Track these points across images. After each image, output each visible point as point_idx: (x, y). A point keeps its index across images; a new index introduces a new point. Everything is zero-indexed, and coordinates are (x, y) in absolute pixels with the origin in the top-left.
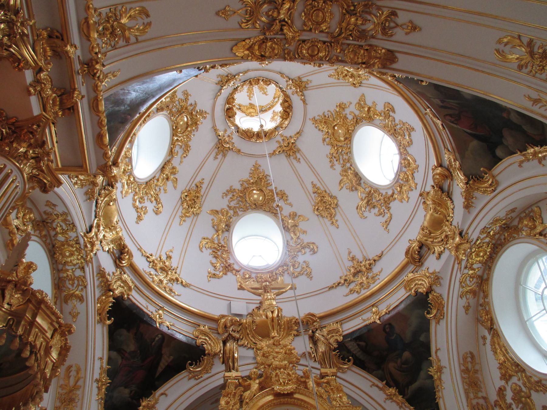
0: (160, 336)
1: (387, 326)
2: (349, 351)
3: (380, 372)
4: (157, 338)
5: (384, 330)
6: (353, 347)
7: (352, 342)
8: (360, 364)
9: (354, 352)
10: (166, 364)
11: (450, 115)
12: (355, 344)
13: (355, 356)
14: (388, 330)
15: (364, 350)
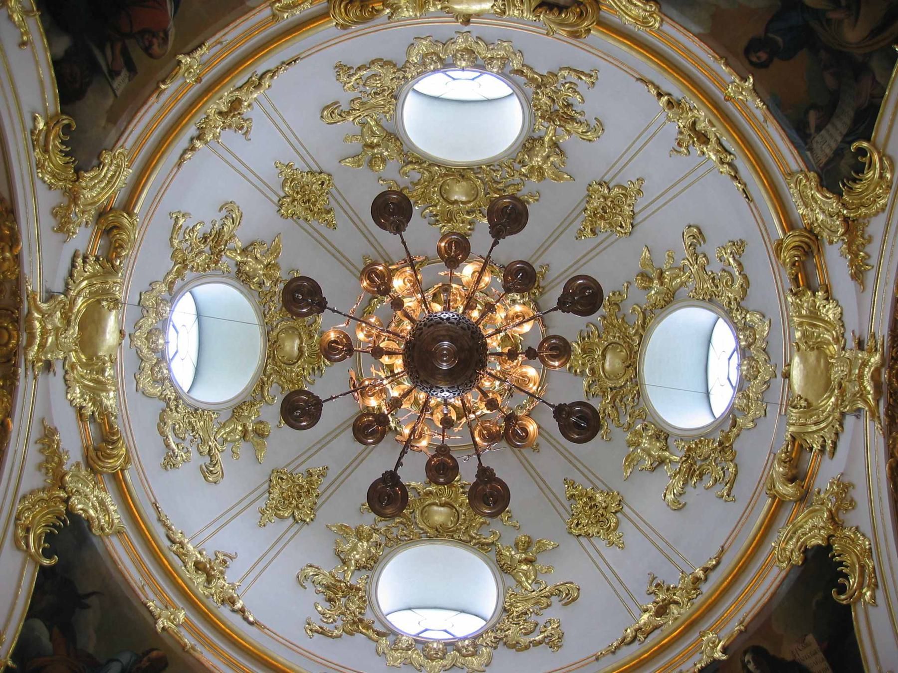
0: (748, 658)
1: (754, 59)
2: (839, 153)
3: (876, 65)
4: (751, 666)
5: (764, 65)
6: (826, 143)
7: (815, 146)
8: (865, 121)
9: (839, 139)
10: (820, 655)
11: (147, 50)
12: (818, 138)
13: (847, 135)
14: (763, 56)
15: (828, 112)
